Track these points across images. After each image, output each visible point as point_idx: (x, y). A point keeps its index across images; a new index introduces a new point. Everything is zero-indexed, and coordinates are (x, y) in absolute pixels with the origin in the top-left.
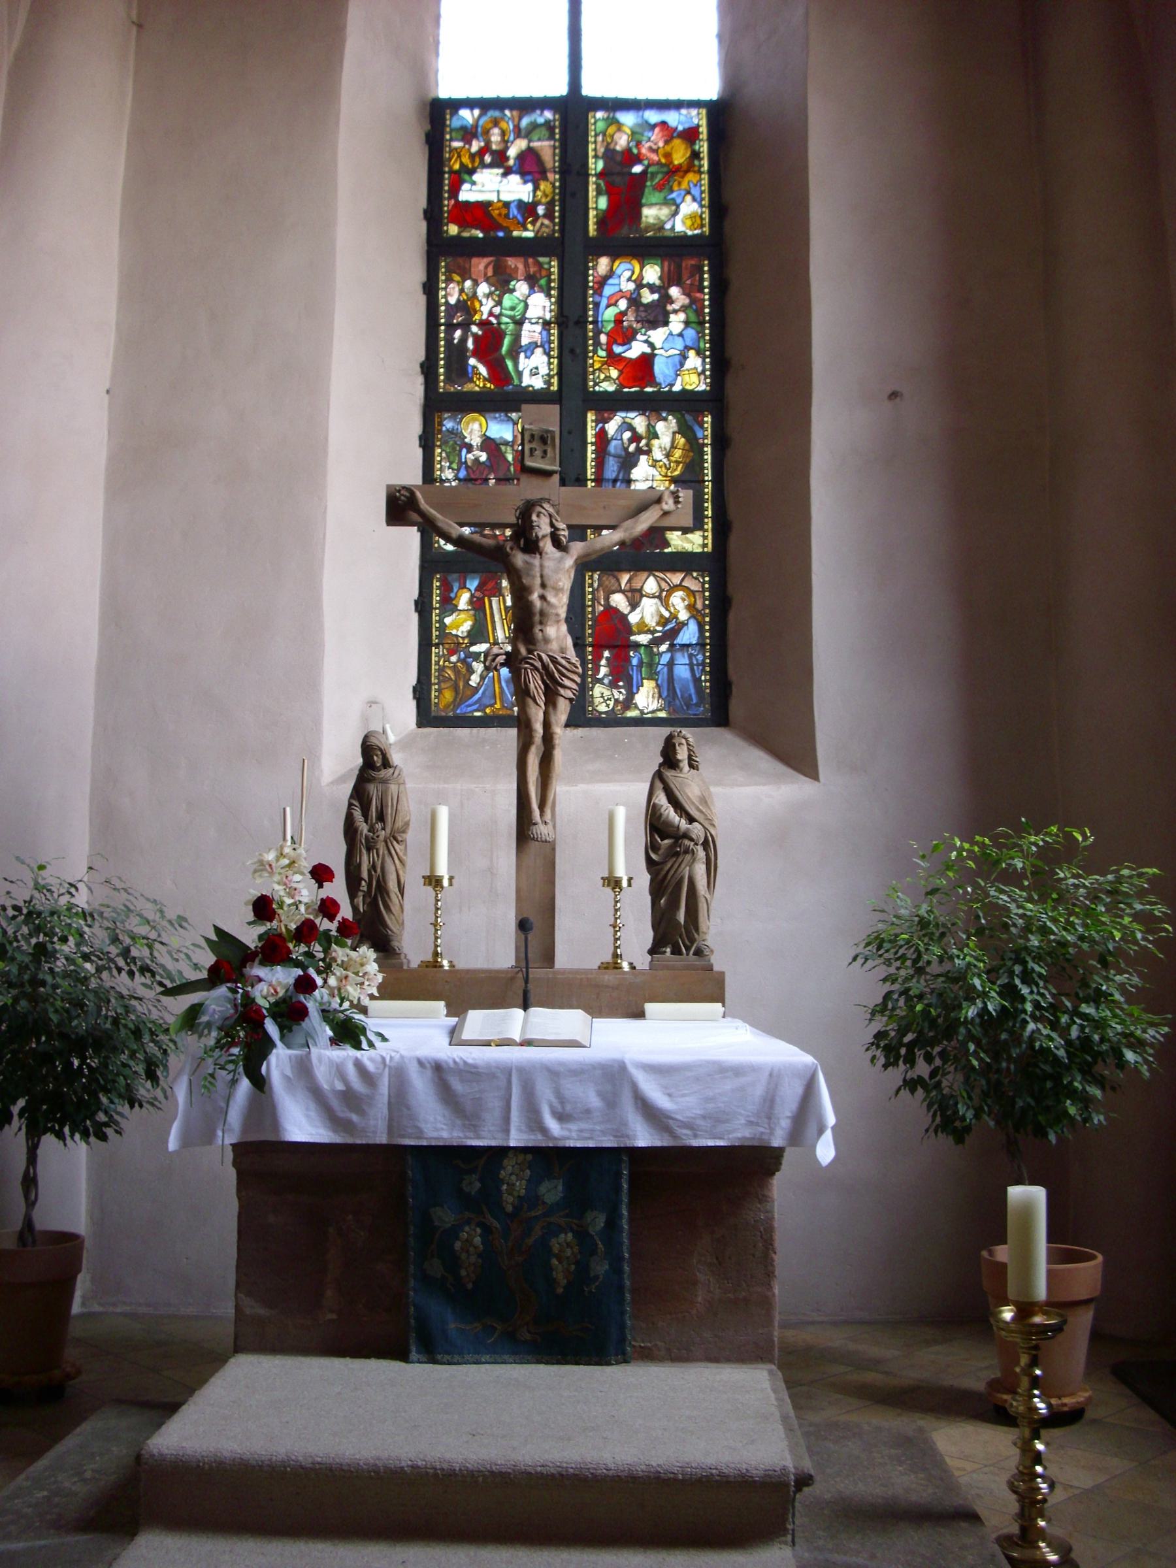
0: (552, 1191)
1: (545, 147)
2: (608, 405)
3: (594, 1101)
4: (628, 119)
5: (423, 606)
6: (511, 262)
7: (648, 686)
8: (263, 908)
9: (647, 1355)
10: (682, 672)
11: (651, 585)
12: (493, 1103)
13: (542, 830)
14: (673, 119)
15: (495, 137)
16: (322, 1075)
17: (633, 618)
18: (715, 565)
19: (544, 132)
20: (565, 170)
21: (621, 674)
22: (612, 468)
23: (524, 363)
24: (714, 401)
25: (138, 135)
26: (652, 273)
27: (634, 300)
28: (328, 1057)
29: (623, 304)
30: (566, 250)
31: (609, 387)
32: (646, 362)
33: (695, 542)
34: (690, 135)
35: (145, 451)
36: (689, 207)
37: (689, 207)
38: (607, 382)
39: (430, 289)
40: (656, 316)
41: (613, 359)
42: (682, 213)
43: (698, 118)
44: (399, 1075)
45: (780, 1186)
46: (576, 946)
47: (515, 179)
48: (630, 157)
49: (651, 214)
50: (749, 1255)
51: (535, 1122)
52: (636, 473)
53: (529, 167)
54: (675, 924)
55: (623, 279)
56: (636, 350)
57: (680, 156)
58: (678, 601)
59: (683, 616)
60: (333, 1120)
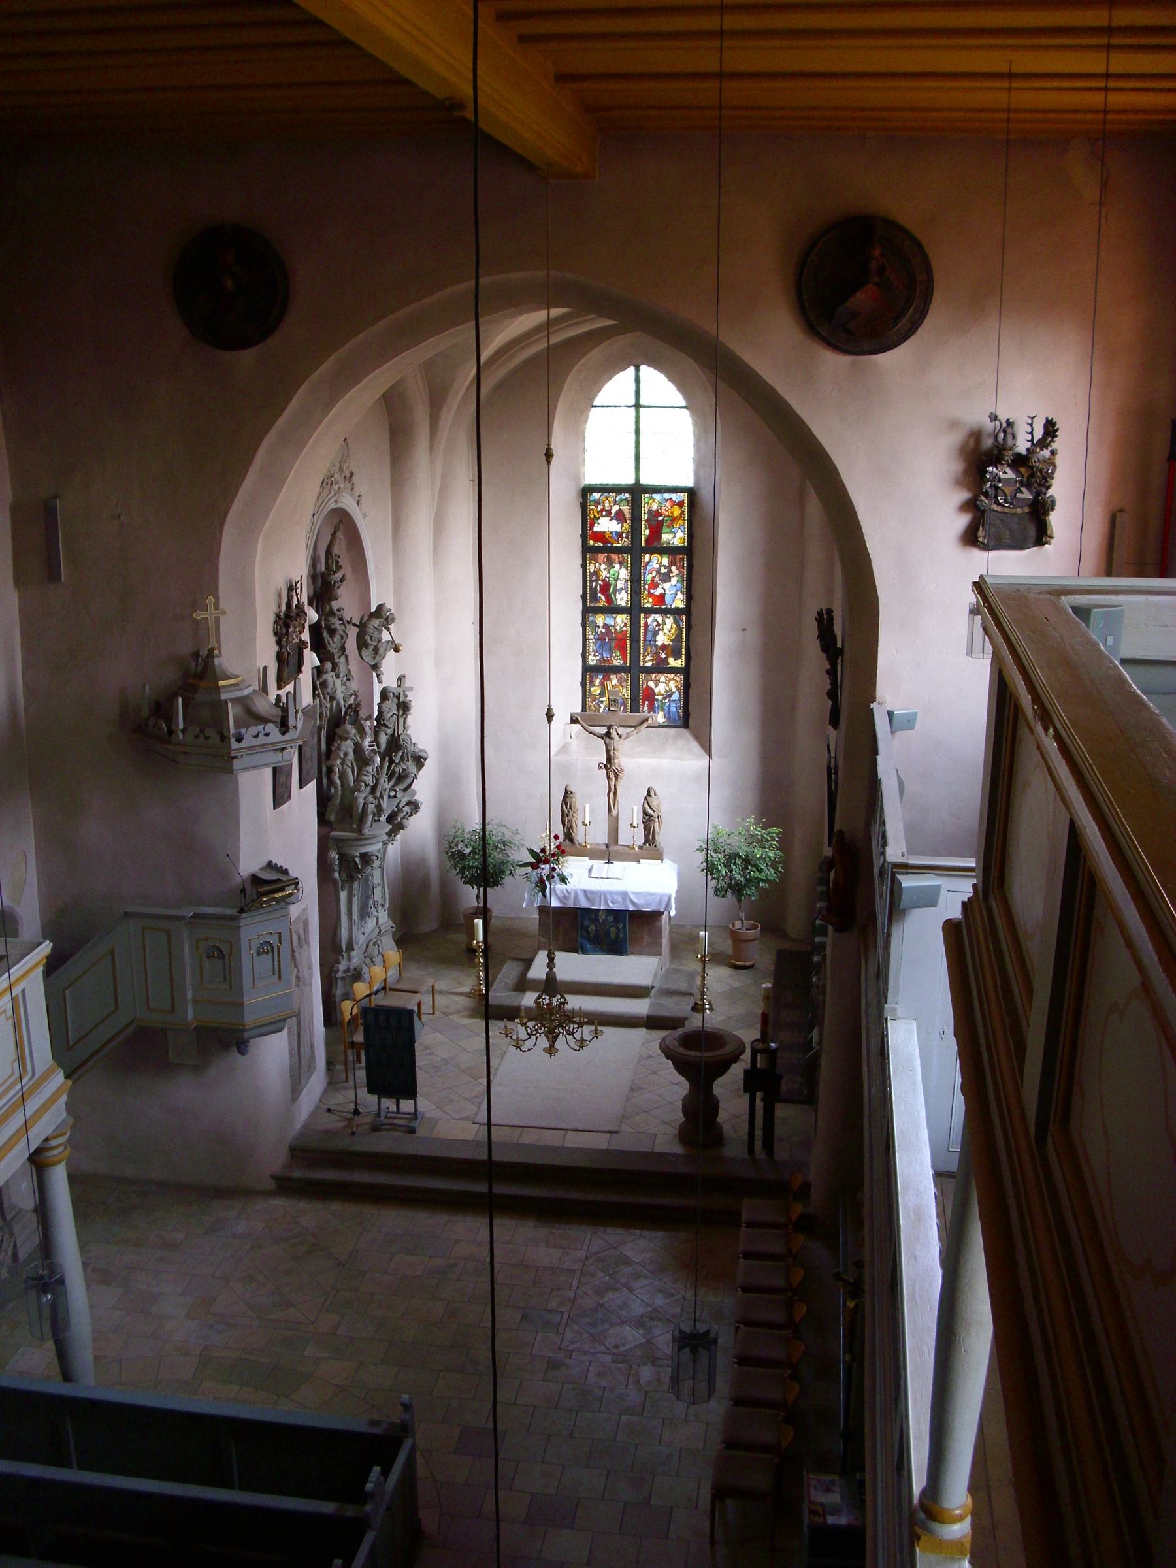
0: (611, 918)
1: (626, 510)
2: (649, 612)
3: (620, 899)
4: (657, 497)
5: (583, 684)
6: (613, 556)
8: (543, 850)
9: (632, 953)
10: (673, 709)
11: (663, 679)
12: (597, 899)
13: (614, 813)
14: (675, 497)
15: (607, 504)
16: (558, 892)
17: (656, 690)
18: (686, 672)
19: (625, 503)
20: (633, 520)
21: (652, 709)
22: (649, 635)
23: (618, 596)
24: (687, 611)
26: (665, 561)
27: (659, 572)
28: (560, 886)
29: (654, 573)
30: (635, 551)
31: (649, 605)
32: (662, 596)
34: (681, 504)
36: (680, 535)
39: (584, 566)
40: (666, 578)
42: (676, 537)
43: (683, 497)
44: (576, 893)
47: (614, 522)
48: (658, 514)
49: (665, 537)
50: (657, 934)
51: (607, 903)
52: (658, 638)
53: (620, 517)
54: (650, 838)
55: (655, 563)
56: (659, 591)
57: (676, 512)
58: (672, 684)
59: (674, 689)
60: (561, 902)
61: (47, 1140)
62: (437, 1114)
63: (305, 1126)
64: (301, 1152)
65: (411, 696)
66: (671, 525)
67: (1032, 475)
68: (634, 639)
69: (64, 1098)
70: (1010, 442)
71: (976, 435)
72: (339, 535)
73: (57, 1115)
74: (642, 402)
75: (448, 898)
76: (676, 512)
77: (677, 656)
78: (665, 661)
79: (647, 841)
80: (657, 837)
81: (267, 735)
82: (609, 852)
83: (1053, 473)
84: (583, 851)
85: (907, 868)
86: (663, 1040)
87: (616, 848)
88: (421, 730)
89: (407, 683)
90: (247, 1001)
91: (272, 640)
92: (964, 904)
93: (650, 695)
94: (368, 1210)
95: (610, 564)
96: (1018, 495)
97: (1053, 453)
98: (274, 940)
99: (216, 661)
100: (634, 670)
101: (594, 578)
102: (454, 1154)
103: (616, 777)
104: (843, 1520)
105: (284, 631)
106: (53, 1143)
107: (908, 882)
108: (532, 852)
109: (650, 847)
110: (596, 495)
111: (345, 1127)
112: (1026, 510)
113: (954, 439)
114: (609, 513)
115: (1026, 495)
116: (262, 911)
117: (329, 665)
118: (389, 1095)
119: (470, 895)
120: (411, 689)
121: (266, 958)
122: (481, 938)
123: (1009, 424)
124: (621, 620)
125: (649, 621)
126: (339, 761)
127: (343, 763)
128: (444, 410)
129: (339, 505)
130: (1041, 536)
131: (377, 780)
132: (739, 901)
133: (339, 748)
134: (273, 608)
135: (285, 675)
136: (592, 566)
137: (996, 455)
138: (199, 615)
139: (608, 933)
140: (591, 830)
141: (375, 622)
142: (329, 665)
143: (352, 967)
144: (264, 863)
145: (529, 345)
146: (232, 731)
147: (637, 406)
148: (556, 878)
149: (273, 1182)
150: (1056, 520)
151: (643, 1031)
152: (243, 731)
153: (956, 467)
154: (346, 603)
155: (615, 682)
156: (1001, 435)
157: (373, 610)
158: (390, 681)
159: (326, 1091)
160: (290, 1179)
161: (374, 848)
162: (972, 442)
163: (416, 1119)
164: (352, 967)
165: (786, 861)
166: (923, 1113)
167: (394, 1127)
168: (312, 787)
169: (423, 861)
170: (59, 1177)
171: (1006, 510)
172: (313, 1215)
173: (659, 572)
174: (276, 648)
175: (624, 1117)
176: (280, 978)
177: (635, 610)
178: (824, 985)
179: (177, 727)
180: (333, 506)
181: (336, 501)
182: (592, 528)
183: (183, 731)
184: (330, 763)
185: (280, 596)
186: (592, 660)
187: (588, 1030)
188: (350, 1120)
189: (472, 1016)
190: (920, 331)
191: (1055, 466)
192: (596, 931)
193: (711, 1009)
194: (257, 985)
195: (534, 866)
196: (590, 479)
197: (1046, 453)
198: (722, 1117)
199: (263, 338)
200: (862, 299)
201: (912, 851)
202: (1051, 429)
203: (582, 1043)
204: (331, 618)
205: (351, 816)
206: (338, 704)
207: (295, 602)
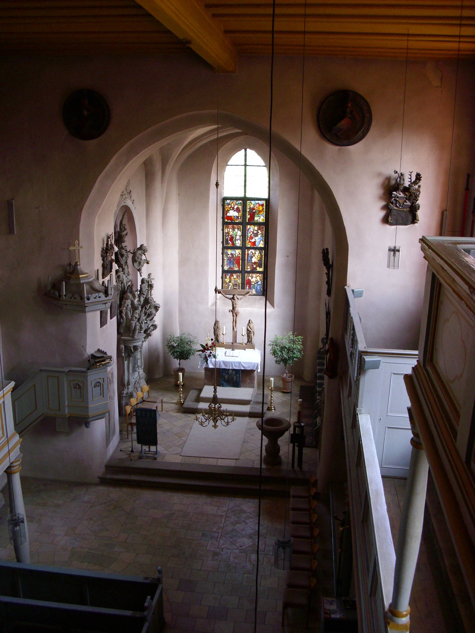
0: (234, 373)
1: (240, 207)
2: (249, 248)
4: (253, 202)
5: (222, 278)
6: (235, 226)
7: (254, 290)
8: (207, 345)
10: (258, 288)
11: (254, 275)
12: (229, 365)
13: (235, 330)
14: (260, 202)
15: (233, 205)
17: (252, 280)
19: (240, 204)
21: (250, 288)
23: (237, 242)
25: (180, 213)
26: (256, 228)
27: (253, 233)
28: (213, 360)
29: (251, 233)
30: (244, 224)
31: (249, 246)
32: (255, 242)
33: (261, 270)
34: (262, 205)
35: (184, 261)
36: (262, 218)
37: (262, 218)
38: (249, 245)
39: (223, 230)
40: (256, 235)
41: (250, 242)
42: (260, 218)
43: (264, 202)
45: (255, 372)
46: (239, 340)
47: (236, 212)
49: (256, 218)
51: (232, 367)
53: (238, 210)
55: (252, 229)
56: (253, 240)
57: (261, 208)
58: (258, 278)
59: (259, 280)
61: (12, 463)
62: (165, 452)
63: (112, 457)
64: (110, 467)
65: (153, 282)
66: (258, 214)
67: (411, 195)
68: (243, 259)
69: (19, 446)
70: (402, 182)
71: (388, 179)
72: (125, 216)
73: (16, 453)
74: (247, 164)
75: (167, 364)
76: (261, 208)
77: (260, 267)
78: (256, 268)
79: (248, 341)
80: (252, 340)
81: (99, 297)
82: (233, 346)
83: (419, 194)
84: (222, 345)
85: (367, 353)
86: (258, 422)
87: (236, 344)
88: (157, 296)
89: (152, 277)
90: (90, 406)
91: (101, 258)
92: (413, 368)
93: (249, 282)
94: (138, 491)
95: (234, 229)
96: (405, 203)
97: (419, 187)
98: (101, 381)
99: (79, 267)
100: (243, 272)
101: (227, 235)
102: (172, 468)
103: (236, 315)
104: (338, 616)
105: (105, 255)
106: (14, 464)
107: (368, 359)
108: (202, 345)
109: (250, 344)
110: (228, 201)
111: (128, 458)
112: (408, 209)
113: (380, 180)
114: (233, 208)
115: (408, 203)
116: (96, 369)
117: (121, 269)
118: (146, 444)
119: (176, 363)
120: (153, 279)
121: (98, 388)
122: (181, 381)
123: (402, 175)
124: (238, 252)
125: (249, 252)
126: (125, 308)
127: (126, 309)
128: (168, 166)
129: (126, 204)
130: (414, 220)
131: (140, 316)
132: (285, 365)
133: (125, 303)
134: (101, 246)
135: (106, 273)
136: (226, 230)
137: (396, 187)
138: (72, 248)
139: (233, 379)
140: (226, 337)
141: (140, 252)
143: (129, 392)
144: (96, 350)
145: (202, 140)
146: (85, 295)
147: (246, 165)
148: (212, 356)
149: (98, 480)
150: (419, 213)
151: (247, 419)
152: (90, 296)
153: (380, 192)
154: (128, 244)
155: (235, 277)
156: (399, 179)
157: (138, 246)
158: (145, 276)
159: (119, 442)
160: (105, 479)
161: (138, 344)
162: (387, 182)
163: (157, 454)
164: (129, 392)
165: (304, 350)
166: (375, 452)
167: (148, 457)
168: (115, 319)
169: (156, 350)
170: (17, 479)
171: (400, 209)
172: (115, 493)
173: (253, 233)
174: (102, 262)
175: (240, 454)
176: (103, 397)
177: (243, 248)
178: (324, 400)
179: (62, 294)
180: (123, 204)
181: (124, 202)
182: (226, 214)
183: (65, 295)
184: (121, 309)
185: (104, 241)
186: (226, 268)
187: (230, 418)
188: (130, 454)
189: (178, 412)
190: (366, 137)
191: (420, 192)
192: (228, 377)
193: (275, 409)
194: (94, 399)
195: (203, 351)
196: (226, 195)
197: (416, 187)
198: (281, 453)
199: (100, 135)
200: (343, 124)
201: (368, 346)
202: (418, 177)
203: (228, 423)
204: (122, 250)
205: (130, 330)
206: (124, 285)
207: (110, 243)
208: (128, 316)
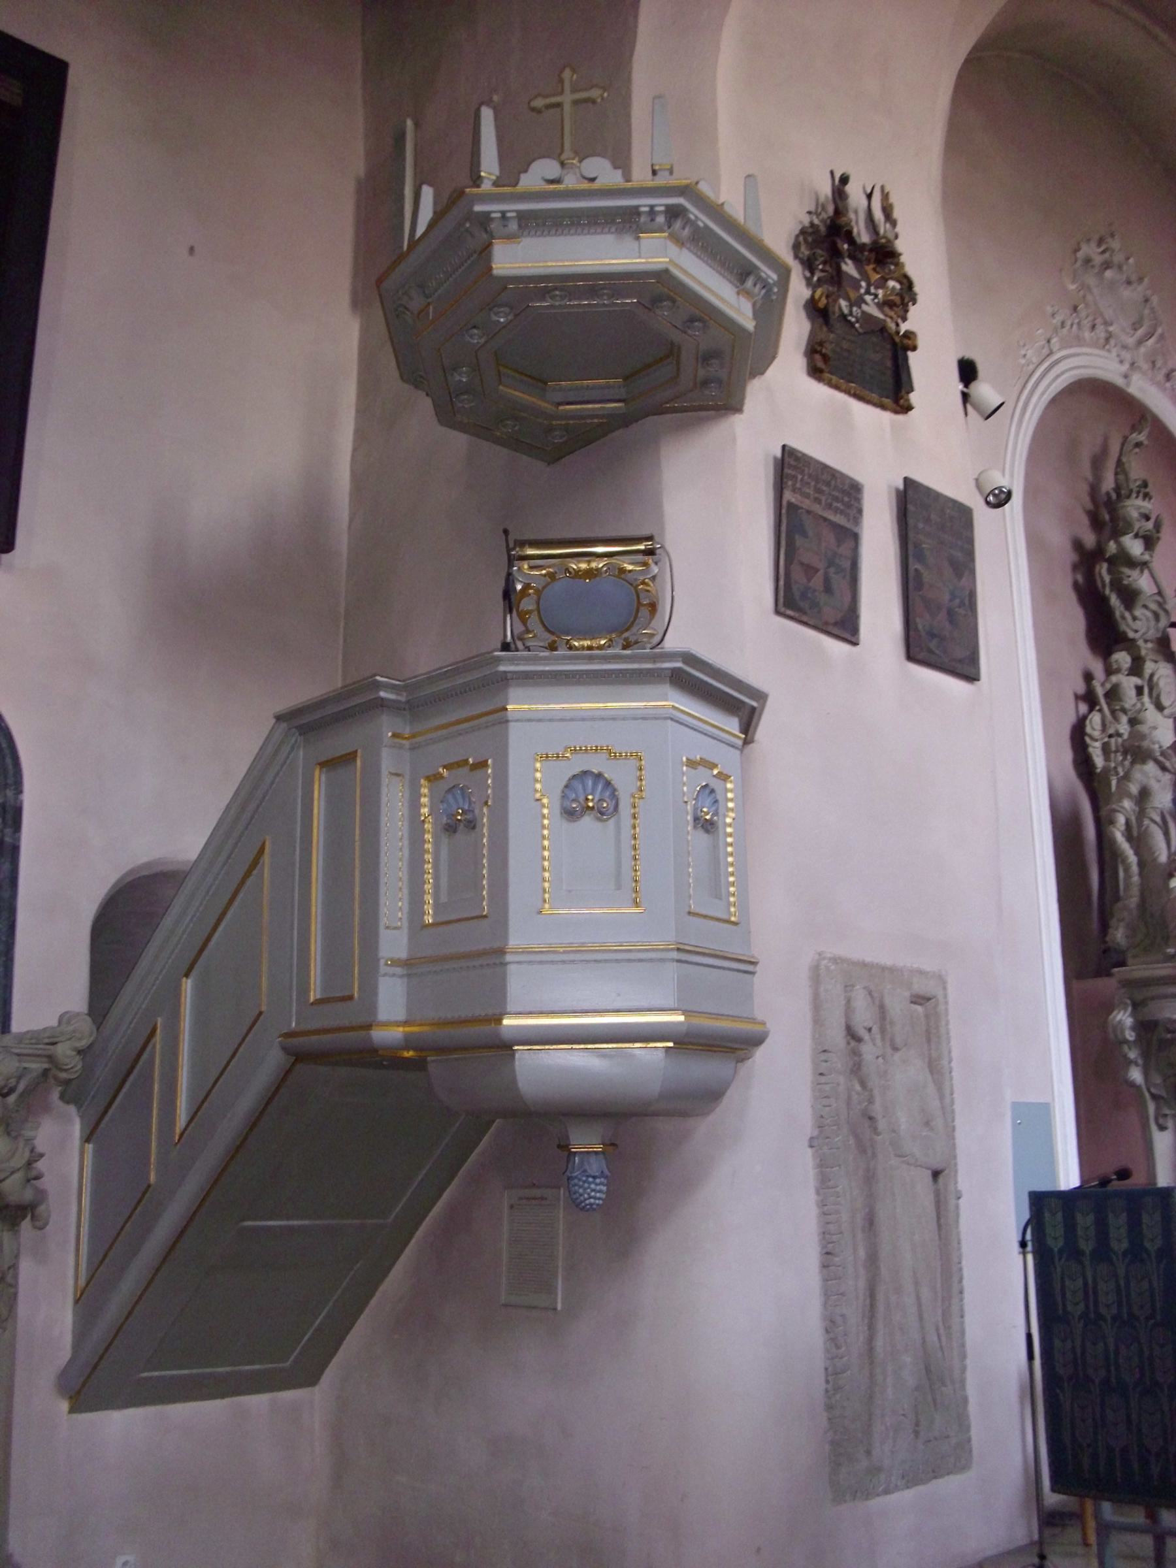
142: (1122, 658)
208: (1151, 850)
